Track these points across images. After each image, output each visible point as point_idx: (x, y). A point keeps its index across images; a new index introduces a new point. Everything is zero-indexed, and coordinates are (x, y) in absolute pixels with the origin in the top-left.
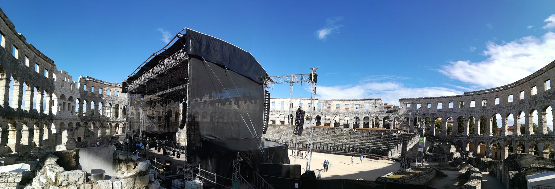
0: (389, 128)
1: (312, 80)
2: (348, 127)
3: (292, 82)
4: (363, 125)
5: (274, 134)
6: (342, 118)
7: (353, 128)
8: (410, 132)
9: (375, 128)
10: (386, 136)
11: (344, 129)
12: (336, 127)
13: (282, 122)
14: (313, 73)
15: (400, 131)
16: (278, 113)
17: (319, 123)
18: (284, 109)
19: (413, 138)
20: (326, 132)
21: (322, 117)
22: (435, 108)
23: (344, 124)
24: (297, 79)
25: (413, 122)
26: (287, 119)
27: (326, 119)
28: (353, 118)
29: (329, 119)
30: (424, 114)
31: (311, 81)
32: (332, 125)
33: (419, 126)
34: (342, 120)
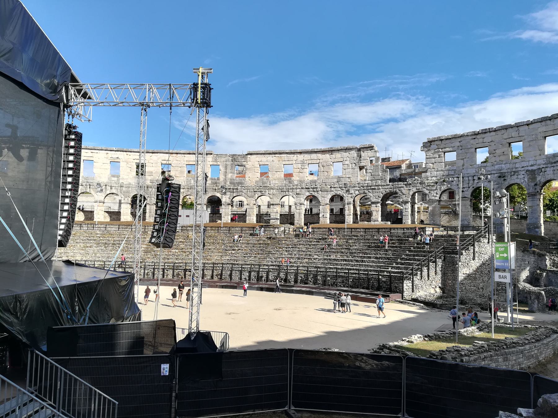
0: (400, 221)
1: (199, 101)
2: (292, 224)
3: (145, 106)
4: (328, 215)
5: (90, 247)
6: (277, 201)
7: (303, 224)
8: (464, 228)
9: (360, 223)
10: (393, 243)
11: (282, 229)
12: (262, 224)
13: (115, 215)
14: (200, 82)
15: (431, 229)
16: (102, 190)
17: (215, 214)
18: (118, 180)
19: (473, 245)
20: (236, 237)
21: (225, 199)
22: (539, 152)
23: (281, 215)
24: (158, 96)
25: (468, 203)
26: (130, 206)
27: (235, 204)
28: (302, 199)
29: (241, 204)
30: (502, 176)
31: (197, 102)
32: (252, 219)
33: (490, 212)
34: (275, 206)
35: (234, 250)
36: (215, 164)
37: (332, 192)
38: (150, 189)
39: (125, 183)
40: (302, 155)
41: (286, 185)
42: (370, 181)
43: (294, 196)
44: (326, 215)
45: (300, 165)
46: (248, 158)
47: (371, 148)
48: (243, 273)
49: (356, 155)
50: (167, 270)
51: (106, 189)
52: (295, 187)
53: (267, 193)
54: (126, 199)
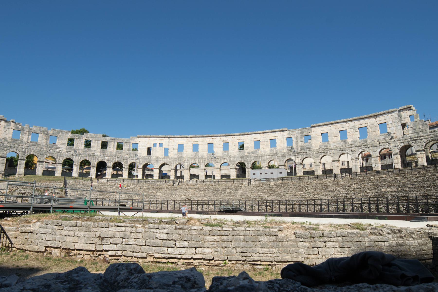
18: (228, 154)
35: (302, 191)
36: (289, 137)
37: (381, 147)
38: (248, 158)
39: (232, 155)
40: (353, 122)
41: (342, 146)
42: (412, 134)
43: (350, 153)
44: (378, 165)
45: (352, 129)
46: (312, 130)
47: (409, 109)
48: (309, 206)
49: (397, 116)
50: (254, 206)
51: (221, 160)
52: (350, 146)
53: (329, 153)
54: (233, 166)
